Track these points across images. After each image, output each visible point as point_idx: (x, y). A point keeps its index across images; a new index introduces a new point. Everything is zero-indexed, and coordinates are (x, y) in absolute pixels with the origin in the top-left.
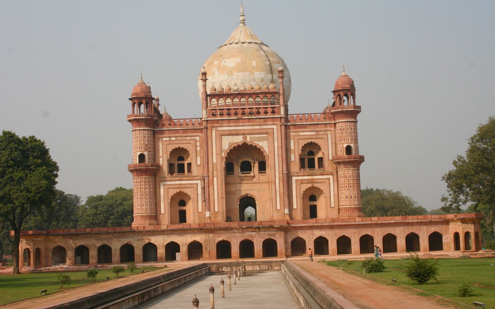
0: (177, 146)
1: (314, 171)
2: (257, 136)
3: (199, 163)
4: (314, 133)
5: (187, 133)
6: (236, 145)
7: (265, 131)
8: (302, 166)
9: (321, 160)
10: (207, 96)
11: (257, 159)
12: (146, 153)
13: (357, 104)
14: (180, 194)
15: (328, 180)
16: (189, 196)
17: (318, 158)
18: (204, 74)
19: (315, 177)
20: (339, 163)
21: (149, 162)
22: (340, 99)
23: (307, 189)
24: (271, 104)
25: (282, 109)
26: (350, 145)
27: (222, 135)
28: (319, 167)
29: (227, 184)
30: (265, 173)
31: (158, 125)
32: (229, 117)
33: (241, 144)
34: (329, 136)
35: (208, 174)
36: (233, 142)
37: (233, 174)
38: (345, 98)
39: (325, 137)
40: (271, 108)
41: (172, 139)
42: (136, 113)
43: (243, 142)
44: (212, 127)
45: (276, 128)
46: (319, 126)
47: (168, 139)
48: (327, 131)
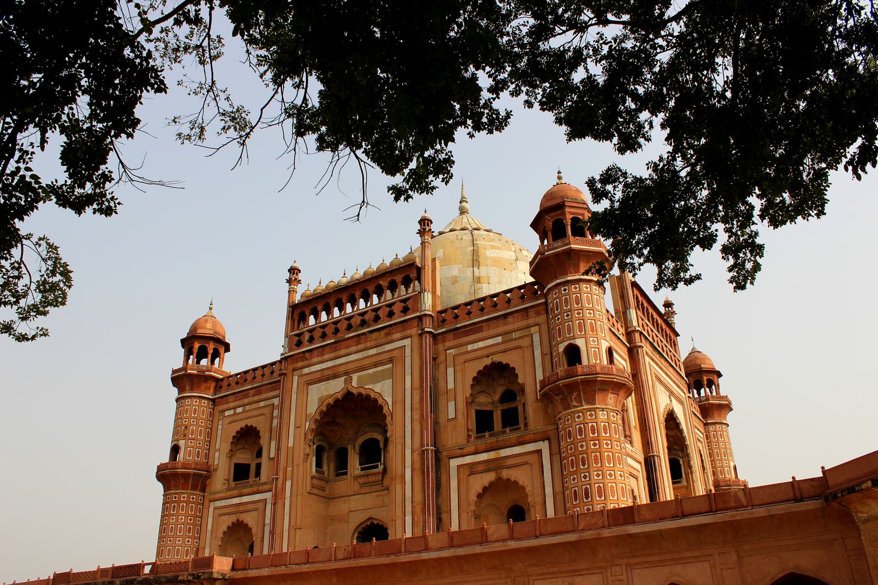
2: (371, 371)
4: (499, 339)
5: (260, 393)
6: (331, 401)
7: (387, 356)
12: (182, 443)
16: (251, 529)
19: (504, 452)
23: (485, 489)
33: (339, 396)
34: (536, 338)
36: (325, 394)
39: (526, 342)
41: (240, 410)
44: (294, 370)
46: (510, 319)
47: (232, 412)
48: (529, 327)
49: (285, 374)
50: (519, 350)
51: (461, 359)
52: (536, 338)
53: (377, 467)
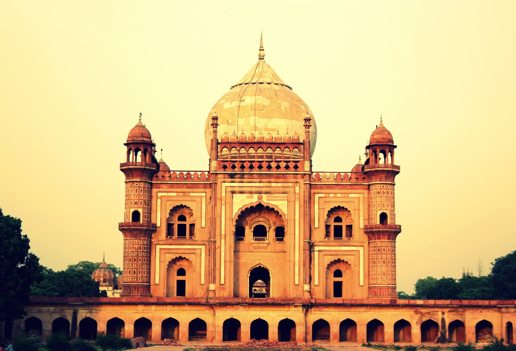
3: (203, 225)
8: (327, 235)
10: (218, 143)
11: (274, 223)
12: (140, 211)
13: (395, 164)
17: (347, 226)
18: (215, 118)
20: (372, 232)
21: (143, 221)
22: (376, 156)
24: (293, 158)
25: (307, 163)
26: (385, 211)
27: (233, 192)
28: (346, 236)
29: (236, 251)
31: (157, 177)
32: (243, 171)
35: (215, 238)
38: (381, 155)
42: (131, 161)
43: (257, 204)
49: (216, 183)
53: (264, 240)
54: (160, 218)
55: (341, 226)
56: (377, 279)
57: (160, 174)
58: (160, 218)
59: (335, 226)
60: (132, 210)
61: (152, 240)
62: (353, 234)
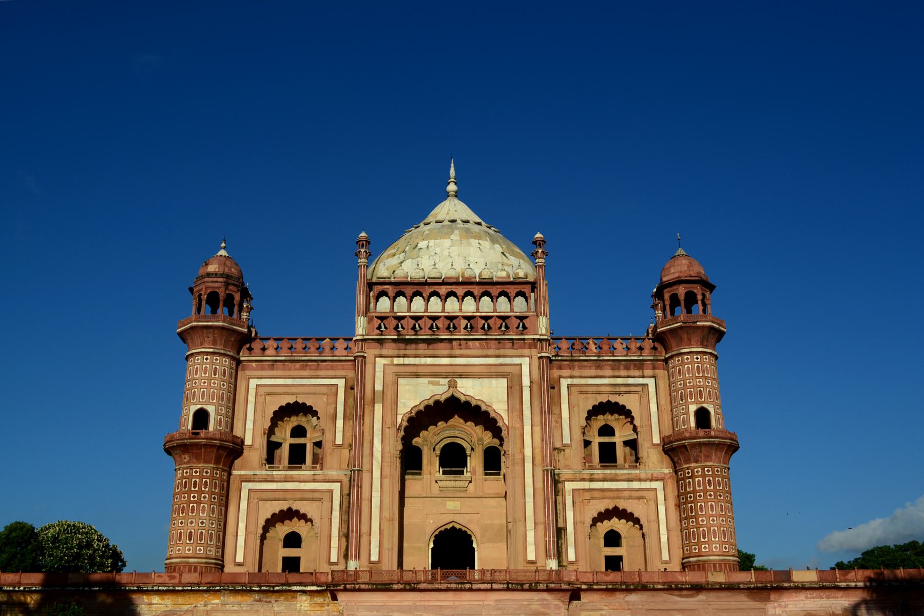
0: (291, 400)
1: (618, 471)
3: (339, 441)
5: (317, 368)
9: (632, 444)
12: (211, 409)
14: (289, 514)
15: (650, 495)
17: (626, 443)
21: (215, 429)
26: (705, 405)
27: (399, 376)
30: (499, 474)
31: (250, 349)
33: (443, 399)
37: (420, 474)
40: (517, 317)
45: (526, 366)
50: (636, 396)
51: (578, 389)
52: (652, 389)
53: (462, 473)
54: (251, 429)
55: (615, 443)
56: (699, 544)
57: (257, 345)
58: (251, 429)
59: (600, 444)
60: (194, 408)
61: (235, 472)
62: (640, 455)
